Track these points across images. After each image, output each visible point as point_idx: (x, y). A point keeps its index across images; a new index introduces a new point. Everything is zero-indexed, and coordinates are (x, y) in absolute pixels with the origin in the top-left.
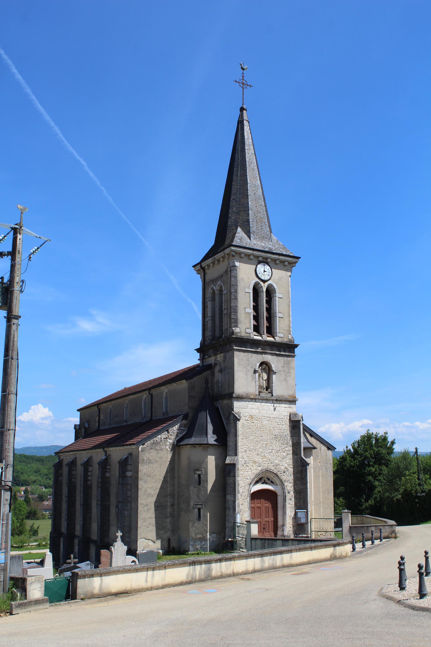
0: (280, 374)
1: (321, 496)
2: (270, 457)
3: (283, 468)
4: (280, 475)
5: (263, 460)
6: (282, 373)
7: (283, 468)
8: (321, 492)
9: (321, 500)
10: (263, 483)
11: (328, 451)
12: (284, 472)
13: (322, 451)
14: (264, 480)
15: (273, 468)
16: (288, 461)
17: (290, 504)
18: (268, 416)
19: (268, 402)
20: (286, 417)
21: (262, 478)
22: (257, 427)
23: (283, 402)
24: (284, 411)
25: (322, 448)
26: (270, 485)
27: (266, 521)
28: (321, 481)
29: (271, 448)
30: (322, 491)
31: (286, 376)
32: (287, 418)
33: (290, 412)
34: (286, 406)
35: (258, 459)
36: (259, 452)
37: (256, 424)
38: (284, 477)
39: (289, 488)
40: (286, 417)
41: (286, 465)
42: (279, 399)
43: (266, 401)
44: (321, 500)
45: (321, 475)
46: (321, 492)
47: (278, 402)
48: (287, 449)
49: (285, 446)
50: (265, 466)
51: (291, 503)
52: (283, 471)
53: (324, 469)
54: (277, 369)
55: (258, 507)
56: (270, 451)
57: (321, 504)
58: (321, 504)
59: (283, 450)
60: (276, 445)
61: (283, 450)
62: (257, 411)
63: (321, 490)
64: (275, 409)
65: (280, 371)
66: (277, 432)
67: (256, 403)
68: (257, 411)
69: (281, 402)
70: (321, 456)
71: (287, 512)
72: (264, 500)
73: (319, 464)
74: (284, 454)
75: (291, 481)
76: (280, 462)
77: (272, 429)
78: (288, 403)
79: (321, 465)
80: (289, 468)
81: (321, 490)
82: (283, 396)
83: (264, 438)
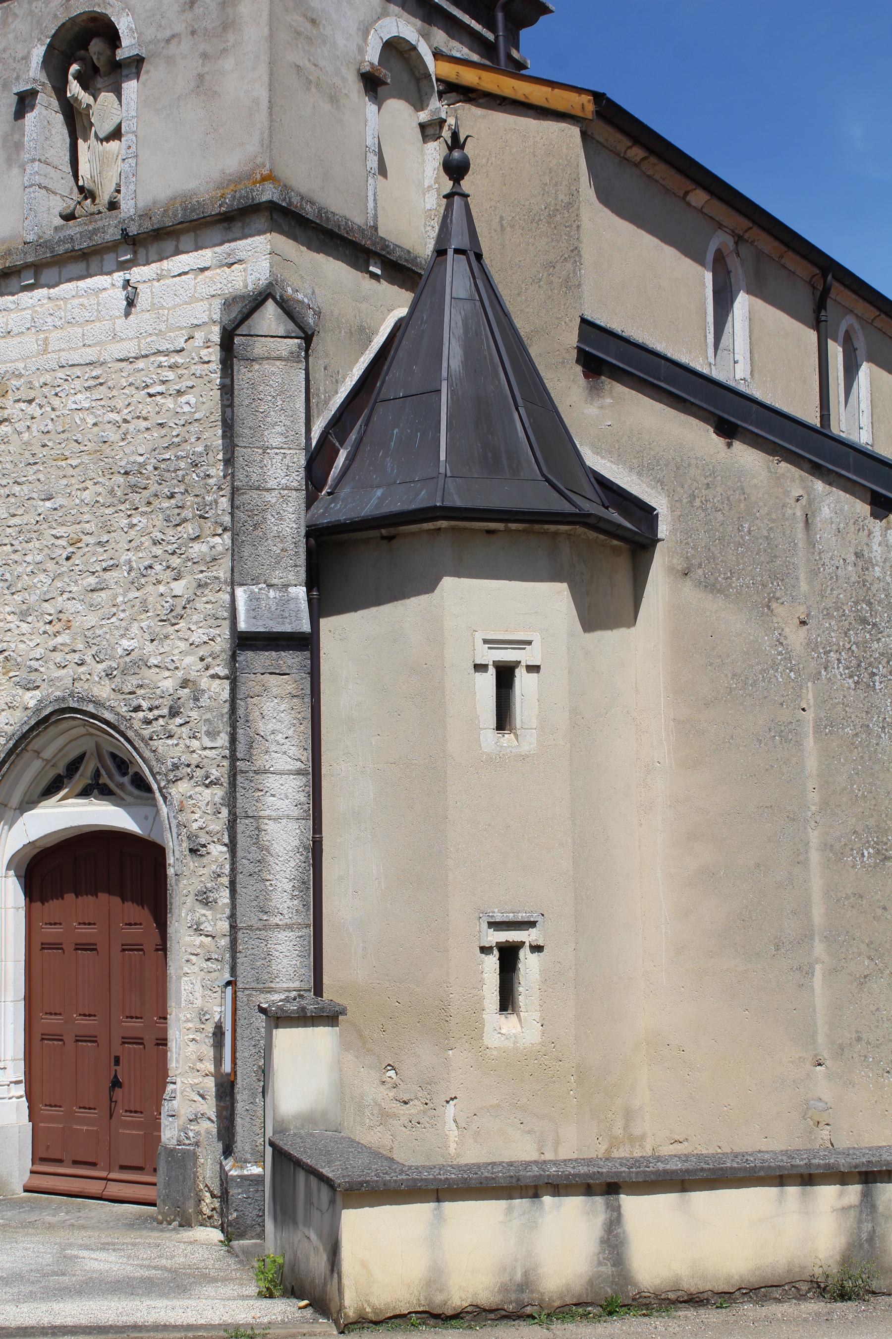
0: (170, 60)
1: (817, 885)
2: (92, 619)
3: (168, 684)
4: (146, 732)
5: (52, 643)
6: (186, 45)
7: (168, 684)
8: (815, 857)
9: (818, 913)
10: (85, 793)
11: (877, 526)
12: (174, 712)
13: (825, 534)
14: (97, 774)
15: (103, 691)
16: (198, 636)
17: (198, 931)
18: (90, 354)
19: (94, 262)
20: (199, 336)
21: (81, 758)
22: (27, 444)
23: (186, 240)
24: (194, 300)
25: (826, 512)
26: (119, 802)
27: (126, 1040)
28: (812, 763)
29: (97, 558)
30: (826, 847)
31: (205, 56)
32: (207, 344)
33: (228, 290)
34: (205, 256)
35: (27, 642)
36: (33, 599)
37: (21, 426)
38: (170, 750)
39: (197, 821)
40: (199, 336)
41: (189, 660)
42: (148, 226)
43: (80, 267)
44: (818, 913)
45: (809, 716)
46: (815, 857)
47: (153, 249)
48: (198, 549)
49: (190, 529)
50: (57, 683)
51: (207, 927)
52: (167, 702)
53: (838, 671)
54: (150, 33)
55: (80, 947)
56: (92, 580)
57: (819, 948)
58: (819, 948)
59: (175, 561)
60: (137, 536)
61: (175, 561)
62: (30, 343)
63: (814, 837)
64: (131, 303)
65: (168, 41)
66: (138, 449)
67: (25, 298)
68: (30, 343)
69: (170, 245)
70: (814, 573)
71: (185, 985)
72: (116, 900)
73: (796, 638)
74: (179, 587)
75: (215, 773)
76: (149, 648)
77: (112, 435)
78: (215, 233)
79: (813, 646)
80: (204, 682)
81: (814, 837)
82: (186, 197)
83: (59, 501)
